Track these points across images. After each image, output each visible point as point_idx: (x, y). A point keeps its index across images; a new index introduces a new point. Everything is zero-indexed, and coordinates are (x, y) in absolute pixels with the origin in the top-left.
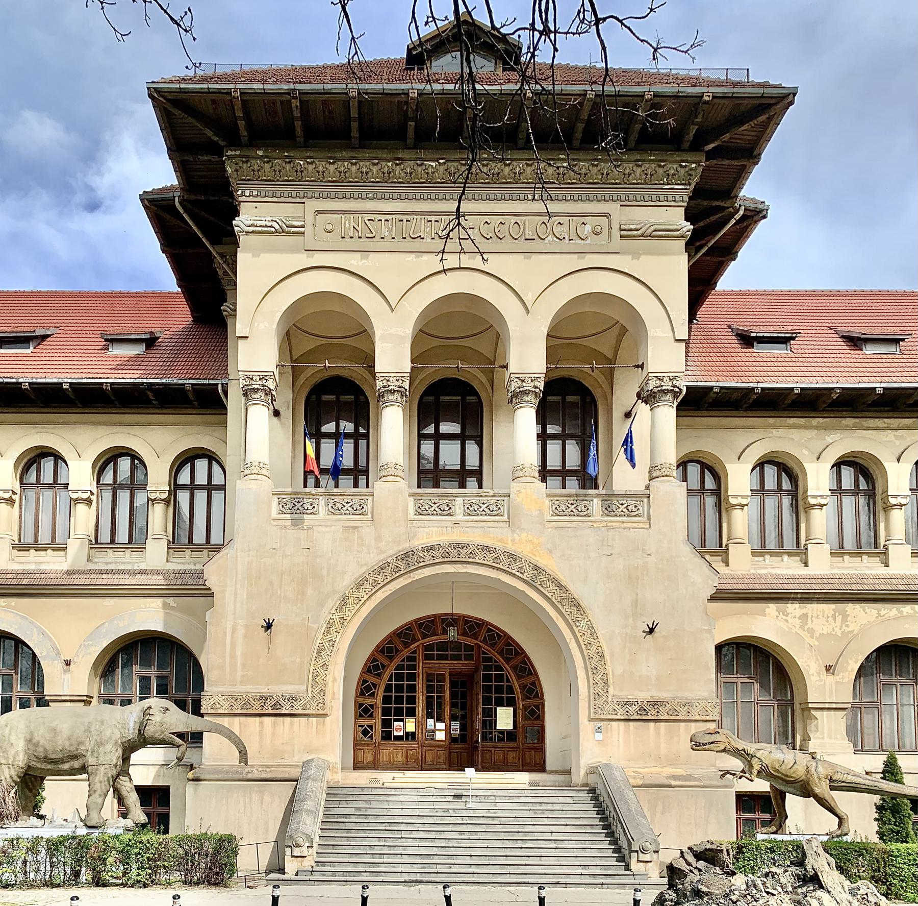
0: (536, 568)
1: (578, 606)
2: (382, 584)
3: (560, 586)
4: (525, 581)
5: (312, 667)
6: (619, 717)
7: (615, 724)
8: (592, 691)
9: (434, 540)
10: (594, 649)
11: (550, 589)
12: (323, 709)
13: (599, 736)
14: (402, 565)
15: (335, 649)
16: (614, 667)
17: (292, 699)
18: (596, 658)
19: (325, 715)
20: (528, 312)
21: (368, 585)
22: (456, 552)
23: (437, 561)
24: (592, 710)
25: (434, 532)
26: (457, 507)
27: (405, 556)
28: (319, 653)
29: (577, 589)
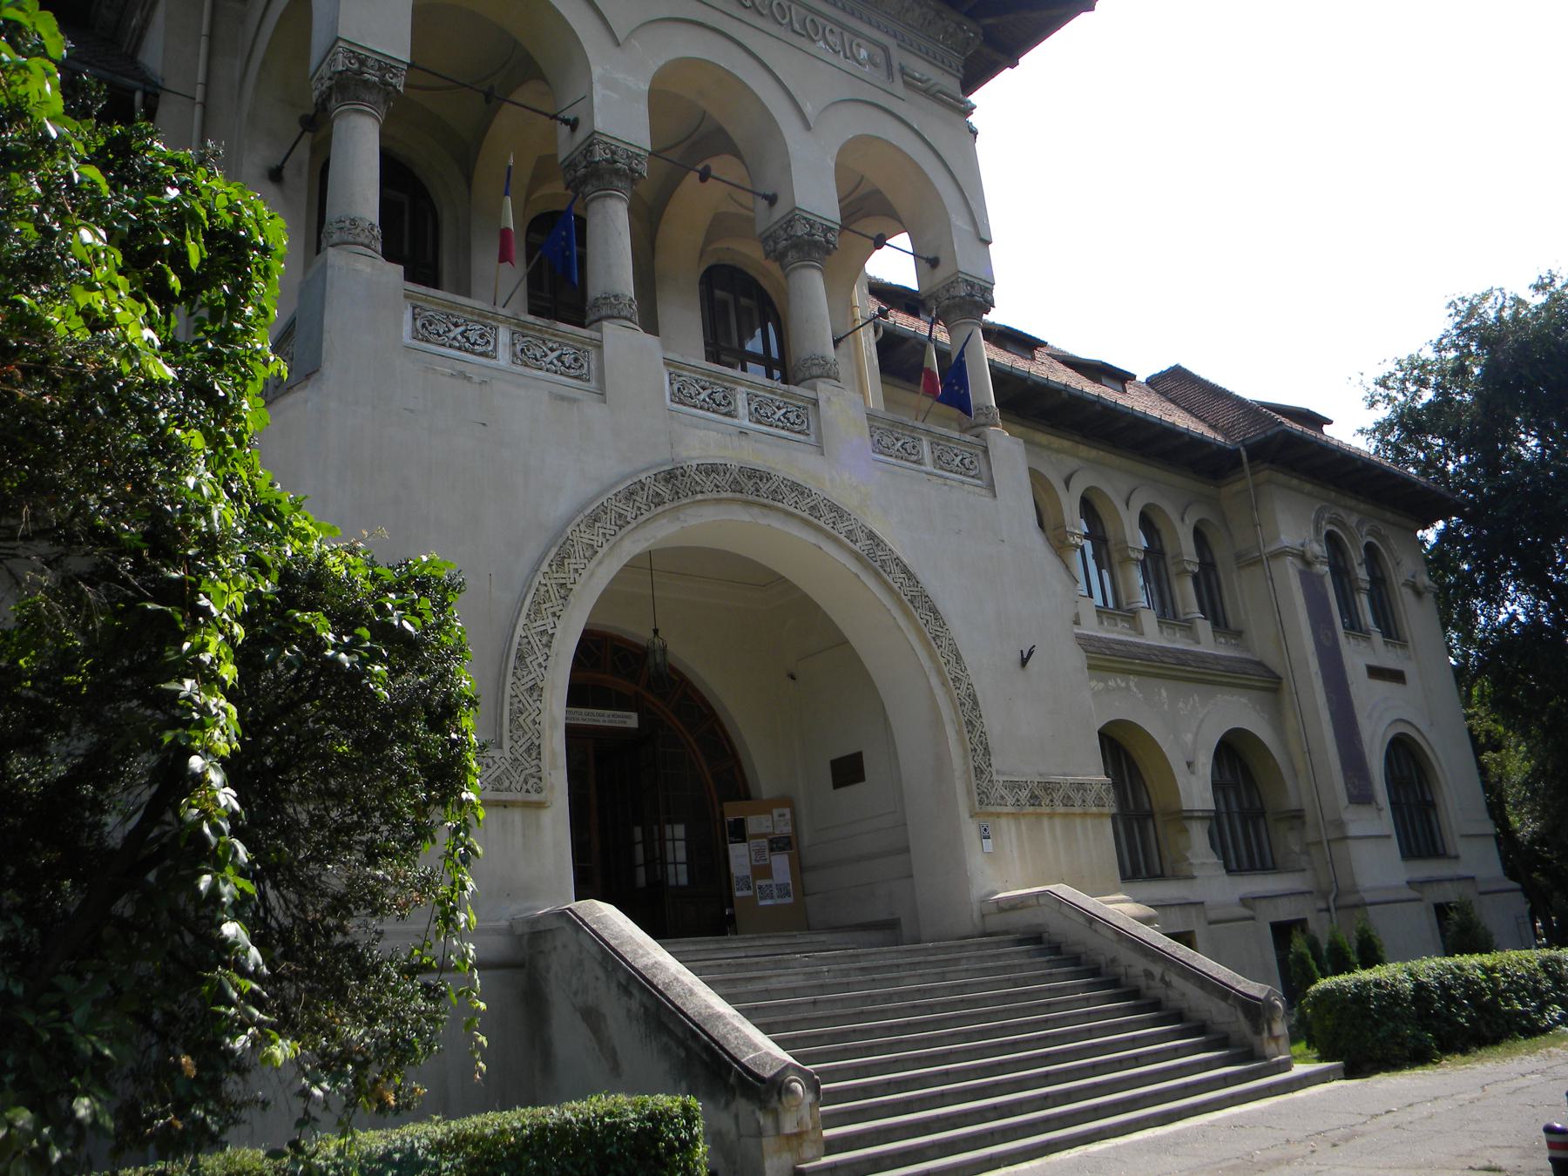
0: (871, 536)
1: (934, 611)
2: (634, 524)
3: (905, 570)
4: (857, 557)
5: (508, 691)
6: (1009, 809)
7: (1003, 821)
8: (971, 763)
9: (715, 455)
10: (963, 686)
11: (895, 578)
12: (539, 791)
13: (988, 844)
14: (665, 491)
15: (552, 652)
16: (993, 722)
18: (969, 704)
19: (540, 805)
20: (808, 127)
22: (750, 485)
23: (724, 495)
24: (976, 798)
25: (706, 440)
26: (740, 404)
27: (670, 477)
28: (521, 658)
29: (931, 583)
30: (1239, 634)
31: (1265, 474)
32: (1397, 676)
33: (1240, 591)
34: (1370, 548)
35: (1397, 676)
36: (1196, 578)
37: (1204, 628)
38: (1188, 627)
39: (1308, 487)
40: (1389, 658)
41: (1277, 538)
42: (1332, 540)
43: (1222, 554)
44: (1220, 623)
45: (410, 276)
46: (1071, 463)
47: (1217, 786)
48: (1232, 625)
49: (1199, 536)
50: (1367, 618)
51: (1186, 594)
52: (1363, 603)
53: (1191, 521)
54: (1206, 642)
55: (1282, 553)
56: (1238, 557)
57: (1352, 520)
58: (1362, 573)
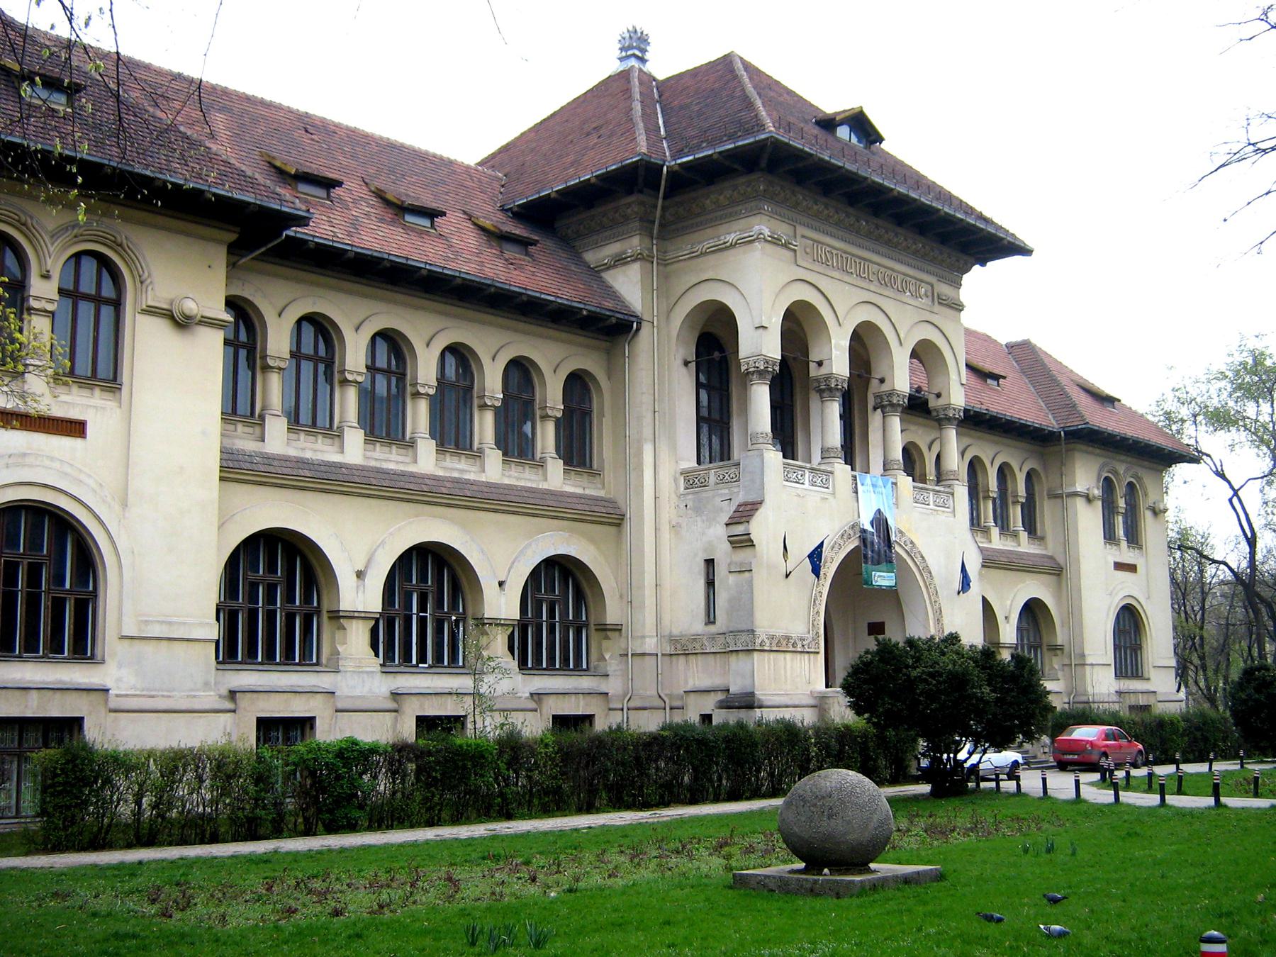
17: (802, 639)
21: (836, 549)
30: (1042, 539)
31: (1072, 446)
32: (1132, 568)
33: (1047, 513)
34: (1131, 485)
35: (1132, 568)
36: (1023, 505)
37: (1024, 535)
38: (1015, 535)
39: (1098, 451)
40: (1128, 555)
41: (1074, 485)
42: (1108, 485)
43: (1041, 490)
44: (1030, 525)
45: (784, 457)
46: (966, 441)
47: (1019, 629)
48: (1039, 533)
49: (1029, 477)
50: (1120, 531)
51: (1016, 514)
52: (1119, 520)
53: (1025, 470)
54: (1024, 545)
55: (1075, 494)
56: (1049, 491)
57: (1121, 469)
58: (1122, 503)
